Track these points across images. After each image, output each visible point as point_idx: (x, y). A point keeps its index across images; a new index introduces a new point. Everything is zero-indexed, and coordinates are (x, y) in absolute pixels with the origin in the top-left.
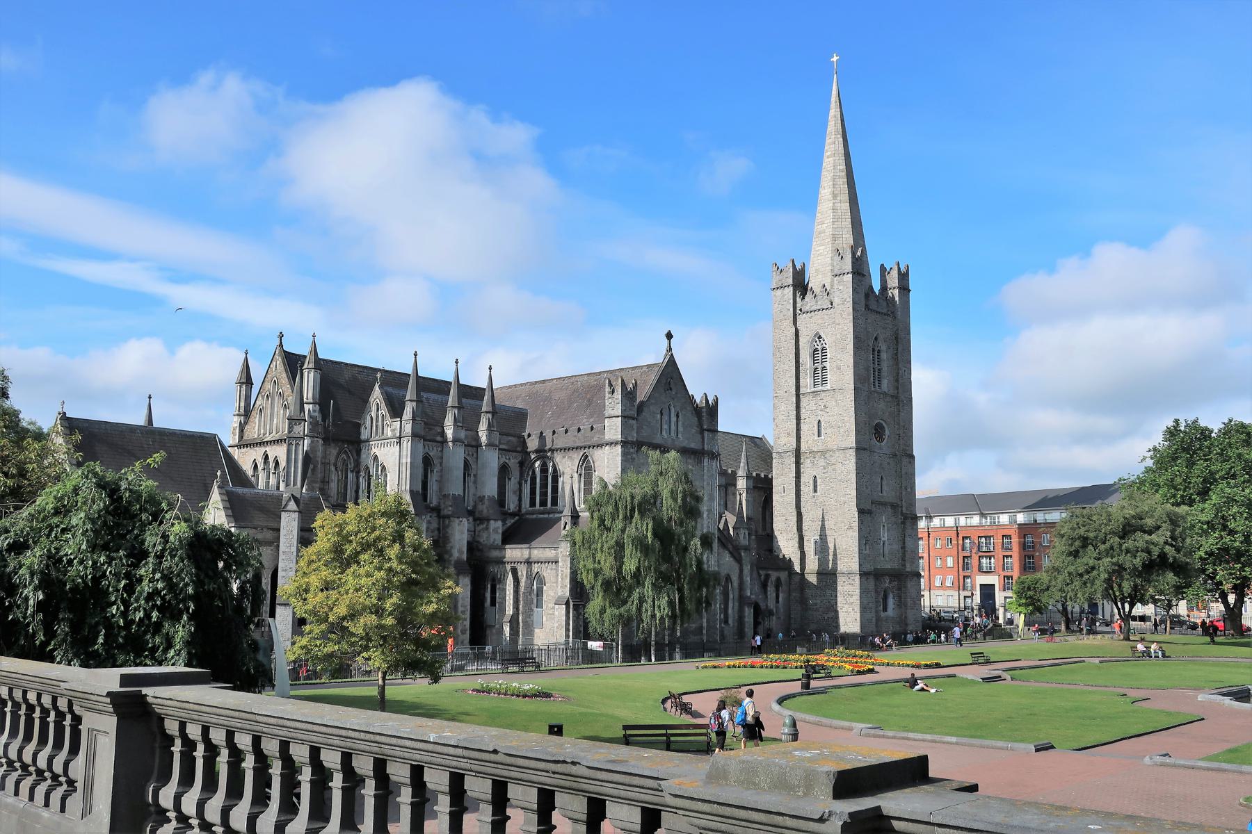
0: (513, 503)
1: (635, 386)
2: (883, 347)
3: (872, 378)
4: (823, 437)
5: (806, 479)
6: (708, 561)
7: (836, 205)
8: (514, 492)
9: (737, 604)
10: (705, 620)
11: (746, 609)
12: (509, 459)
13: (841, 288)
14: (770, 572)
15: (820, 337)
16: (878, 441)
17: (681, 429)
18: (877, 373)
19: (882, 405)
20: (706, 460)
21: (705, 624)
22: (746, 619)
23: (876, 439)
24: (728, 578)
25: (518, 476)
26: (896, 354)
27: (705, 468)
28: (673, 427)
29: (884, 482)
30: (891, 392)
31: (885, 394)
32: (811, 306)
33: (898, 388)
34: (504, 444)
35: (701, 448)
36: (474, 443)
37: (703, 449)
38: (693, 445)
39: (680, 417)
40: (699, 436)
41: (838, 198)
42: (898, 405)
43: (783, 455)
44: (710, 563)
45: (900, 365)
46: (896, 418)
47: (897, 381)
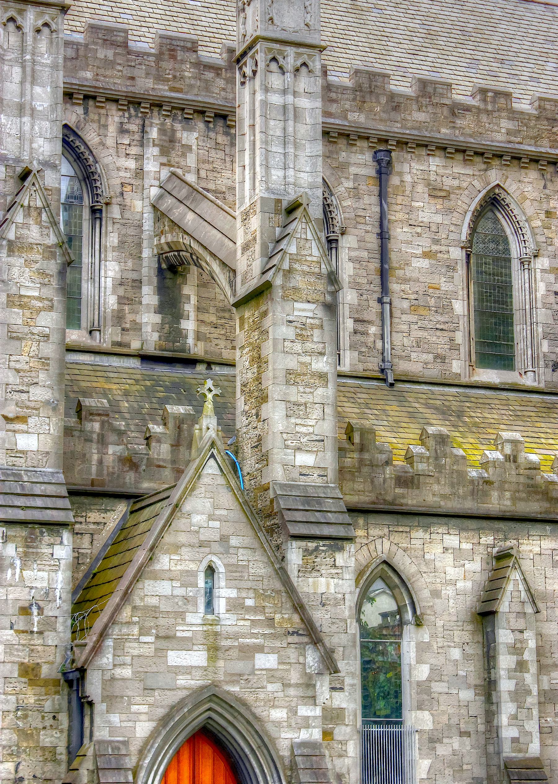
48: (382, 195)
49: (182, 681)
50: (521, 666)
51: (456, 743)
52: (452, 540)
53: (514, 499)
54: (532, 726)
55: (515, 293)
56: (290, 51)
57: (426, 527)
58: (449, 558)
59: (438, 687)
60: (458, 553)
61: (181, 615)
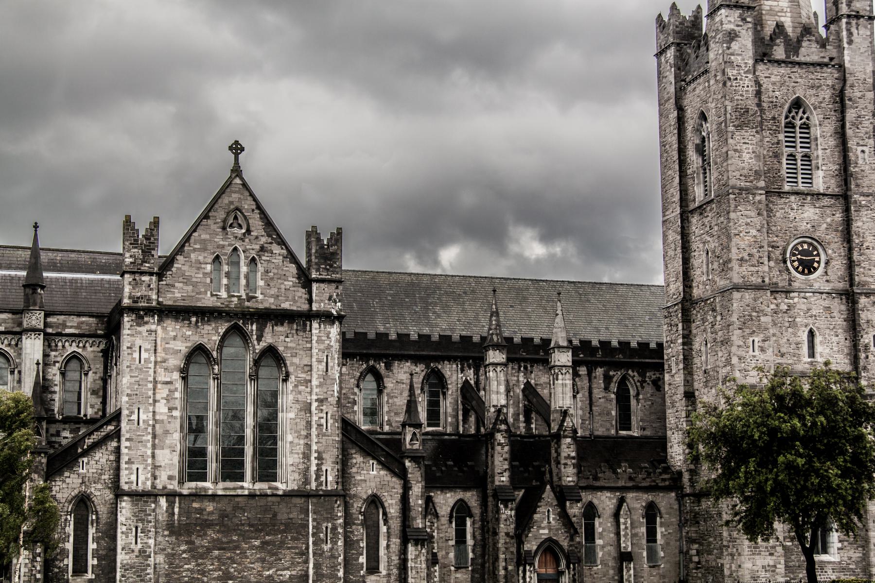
0: (92, 407)
4: (710, 277)
6: (318, 477)
8: (94, 392)
9: (396, 541)
10: (311, 565)
11: (411, 548)
12: (84, 346)
14: (630, 496)
16: (803, 273)
20: (315, 325)
21: (311, 572)
22: (410, 564)
23: (796, 269)
24: (375, 501)
25: (102, 369)
26: (843, 126)
27: (315, 338)
29: (818, 339)
30: (834, 189)
31: (818, 195)
34: (71, 327)
35: (305, 307)
36: (18, 329)
38: (286, 305)
40: (304, 290)
42: (847, 210)
44: (323, 479)
45: (851, 144)
48: (590, 381)
49: (544, 537)
50: (626, 528)
51: (609, 548)
52: (608, 494)
53: (625, 483)
54: (629, 544)
55: (632, 407)
56: (564, 368)
57: (601, 492)
58: (607, 499)
59: (604, 533)
60: (610, 498)
61: (542, 522)
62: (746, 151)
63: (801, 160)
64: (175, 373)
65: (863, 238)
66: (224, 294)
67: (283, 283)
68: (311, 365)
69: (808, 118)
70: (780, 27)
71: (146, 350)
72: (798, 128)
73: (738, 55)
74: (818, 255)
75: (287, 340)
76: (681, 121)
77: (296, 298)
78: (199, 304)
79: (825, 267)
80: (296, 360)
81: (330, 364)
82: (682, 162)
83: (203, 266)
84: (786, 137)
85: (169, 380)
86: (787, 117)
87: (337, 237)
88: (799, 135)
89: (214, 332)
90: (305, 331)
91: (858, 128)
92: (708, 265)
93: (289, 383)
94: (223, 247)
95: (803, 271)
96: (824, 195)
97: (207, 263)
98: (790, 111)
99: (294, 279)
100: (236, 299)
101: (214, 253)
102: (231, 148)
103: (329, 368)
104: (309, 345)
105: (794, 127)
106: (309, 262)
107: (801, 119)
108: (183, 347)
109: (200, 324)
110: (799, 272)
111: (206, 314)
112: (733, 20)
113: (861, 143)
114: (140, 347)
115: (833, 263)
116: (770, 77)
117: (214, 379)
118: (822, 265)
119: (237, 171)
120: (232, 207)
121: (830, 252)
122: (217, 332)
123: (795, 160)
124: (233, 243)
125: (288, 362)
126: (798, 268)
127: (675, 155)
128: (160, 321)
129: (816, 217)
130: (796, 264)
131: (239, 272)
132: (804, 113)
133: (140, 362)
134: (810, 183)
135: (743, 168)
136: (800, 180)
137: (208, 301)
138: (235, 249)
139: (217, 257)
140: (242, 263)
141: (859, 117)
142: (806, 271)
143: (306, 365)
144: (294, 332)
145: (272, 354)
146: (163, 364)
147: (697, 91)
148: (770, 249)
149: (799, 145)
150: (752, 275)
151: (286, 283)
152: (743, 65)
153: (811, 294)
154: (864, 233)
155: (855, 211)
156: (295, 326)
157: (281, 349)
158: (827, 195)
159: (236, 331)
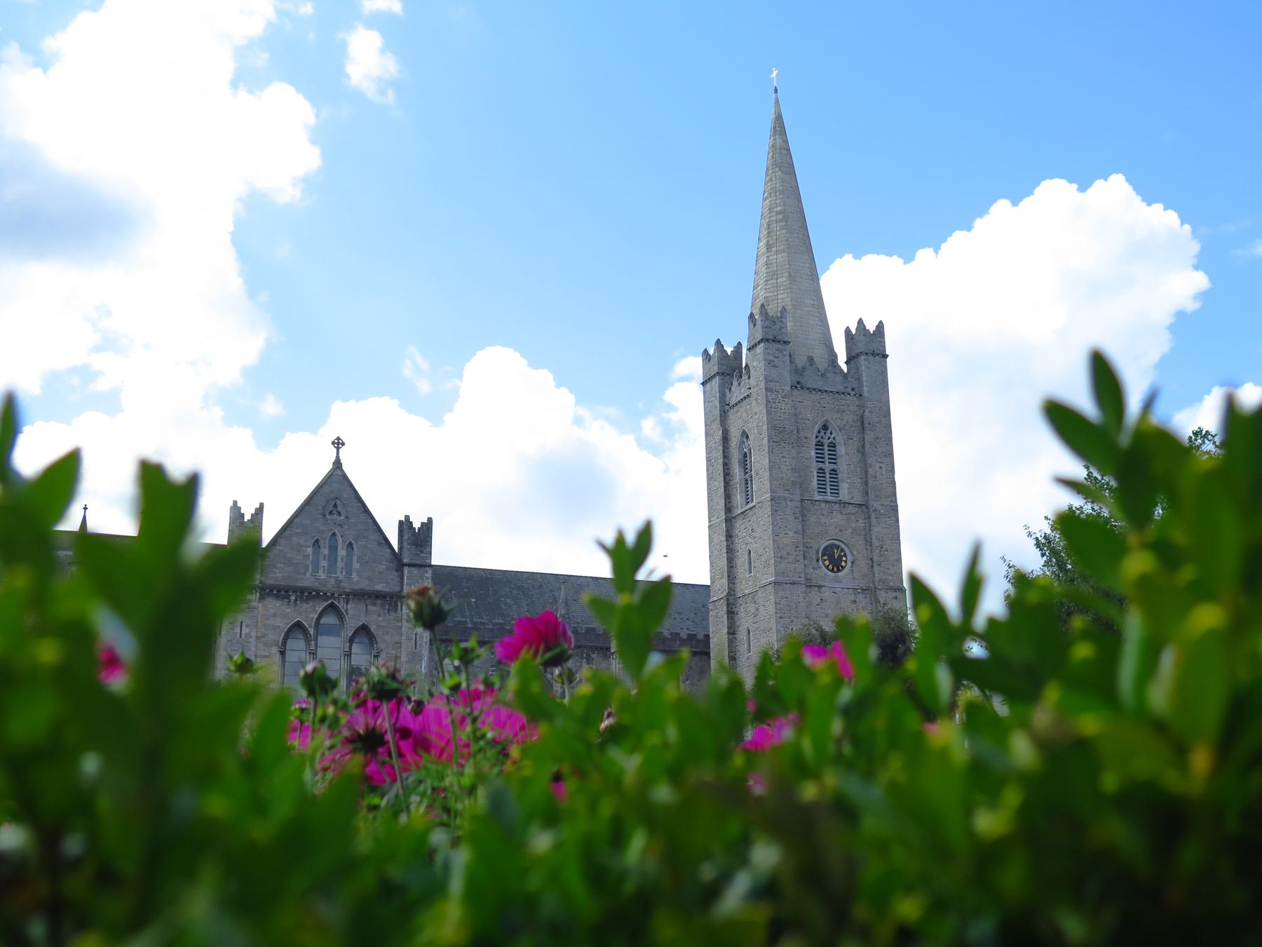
1: (260, 511)
2: (840, 439)
3: (815, 482)
5: (742, 634)
7: (770, 258)
13: (755, 364)
15: (747, 437)
16: (832, 571)
17: (356, 565)
18: (828, 475)
19: (837, 518)
26: (863, 446)
28: (340, 564)
30: (858, 499)
32: (737, 396)
33: (867, 493)
35: (398, 589)
37: (402, 590)
38: (379, 587)
39: (355, 549)
40: (396, 573)
41: (774, 249)
42: (869, 518)
43: (716, 603)
46: (868, 535)
47: (866, 484)
62: (784, 464)
63: (830, 474)
64: (274, 647)
65: (883, 542)
66: (322, 575)
67: (377, 567)
68: (401, 643)
69: (834, 439)
70: (811, 360)
71: (247, 626)
72: (826, 446)
73: (776, 382)
74: (845, 556)
75: (380, 619)
76: (726, 439)
77: (389, 581)
78: (299, 584)
79: (852, 566)
80: (387, 638)
81: (418, 642)
82: (727, 474)
83: (303, 549)
84: (817, 453)
85: (267, 654)
86: (817, 437)
87: (428, 526)
88: (827, 452)
89: (311, 610)
90: (396, 610)
91: (876, 448)
92: (750, 563)
93: (380, 659)
94: (323, 532)
95: (833, 568)
96: (849, 504)
97: (307, 547)
98: (819, 432)
99: (387, 563)
100: (333, 580)
101: (314, 537)
102: (333, 443)
103: (418, 646)
104: (399, 624)
105: (822, 445)
106: (401, 547)
107: (829, 439)
108: (284, 625)
109: (298, 602)
110: (829, 570)
111: (307, 594)
112: (771, 353)
113: (879, 460)
114: (242, 623)
115: (857, 563)
116: (802, 402)
117: (310, 653)
118: (849, 564)
119: (338, 464)
120: (332, 496)
121: (855, 553)
122: (314, 610)
123: (824, 473)
124: (332, 528)
125: (379, 640)
126: (828, 566)
127: (720, 468)
128: (262, 598)
129: (843, 523)
130: (827, 562)
131: (337, 555)
132: (831, 433)
133: (241, 637)
134: (837, 493)
135: (782, 478)
136: (829, 491)
137: (307, 581)
138: (334, 534)
139: (317, 541)
140: (339, 548)
141: (877, 438)
142: (835, 569)
143: (397, 643)
144: (386, 611)
145: (364, 630)
146: (263, 639)
147: (740, 413)
148: (805, 549)
149: (827, 461)
150: (790, 571)
151: (380, 566)
152: (780, 391)
153: (840, 589)
154: (883, 537)
155: (876, 518)
156: (387, 607)
157: (373, 628)
158: (852, 504)
159: (333, 608)
